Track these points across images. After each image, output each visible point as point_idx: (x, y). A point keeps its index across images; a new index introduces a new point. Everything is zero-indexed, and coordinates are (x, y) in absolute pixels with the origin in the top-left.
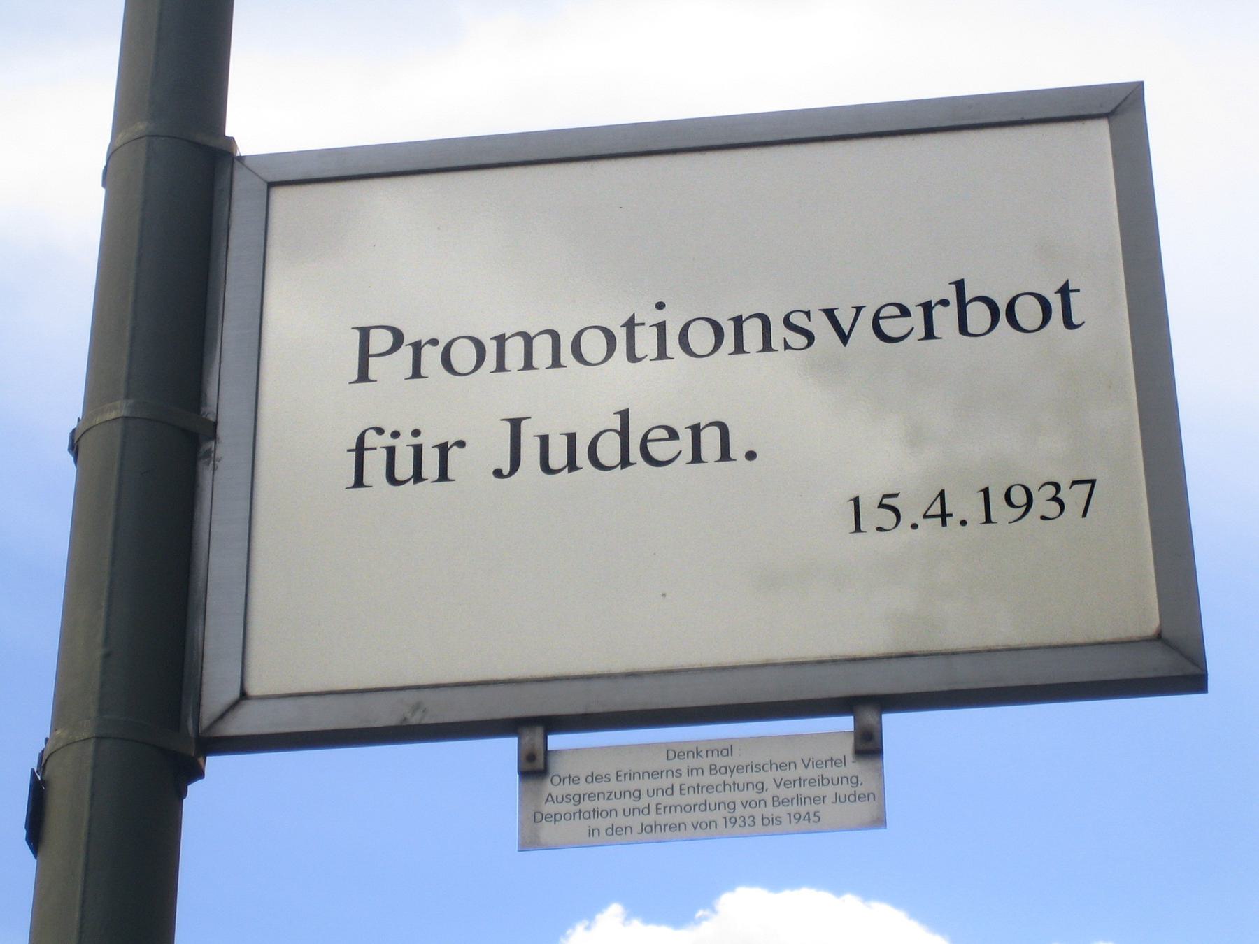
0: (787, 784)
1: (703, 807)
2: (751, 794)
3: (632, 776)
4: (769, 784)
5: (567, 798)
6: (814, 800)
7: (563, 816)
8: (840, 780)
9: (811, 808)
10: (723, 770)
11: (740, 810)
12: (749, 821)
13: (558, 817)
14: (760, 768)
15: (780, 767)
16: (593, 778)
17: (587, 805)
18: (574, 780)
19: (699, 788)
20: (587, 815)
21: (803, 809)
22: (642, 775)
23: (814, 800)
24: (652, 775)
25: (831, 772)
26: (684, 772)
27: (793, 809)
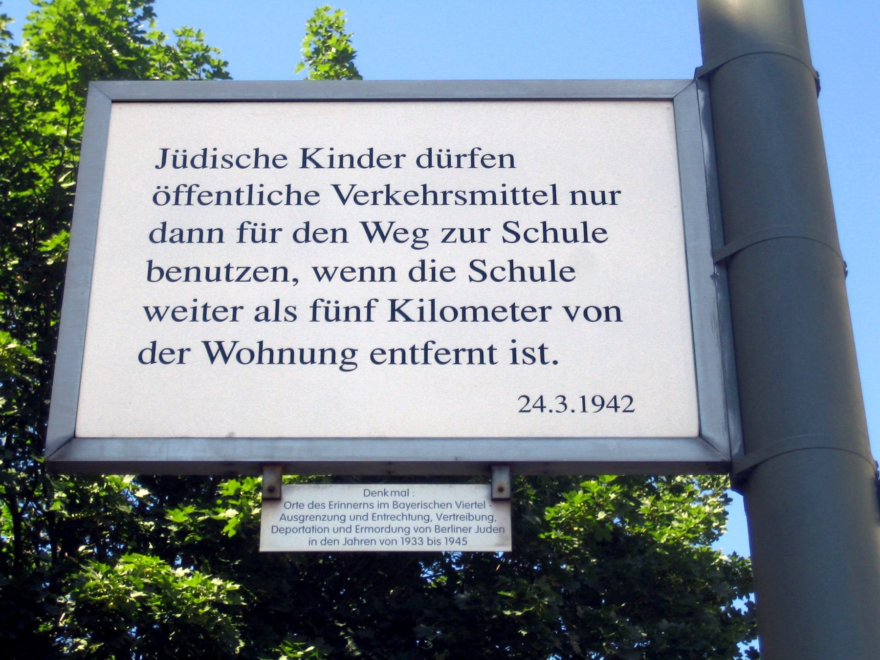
0: (445, 518)
1: (388, 530)
2: (420, 523)
3: (340, 505)
4: (433, 517)
5: (295, 518)
6: (463, 530)
7: (292, 530)
8: (481, 517)
9: (462, 535)
10: (402, 506)
11: (413, 534)
12: (418, 541)
13: (288, 530)
14: (426, 506)
15: (441, 506)
16: (313, 505)
17: (308, 524)
18: (300, 506)
19: (385, 517)
20: (308, 530)
21: (455, 536)
22: (346, 506)
23: (463, 530)
24: (355, 506)
25: (475, 511)
26: (376, 506)
27: (449, 535)
